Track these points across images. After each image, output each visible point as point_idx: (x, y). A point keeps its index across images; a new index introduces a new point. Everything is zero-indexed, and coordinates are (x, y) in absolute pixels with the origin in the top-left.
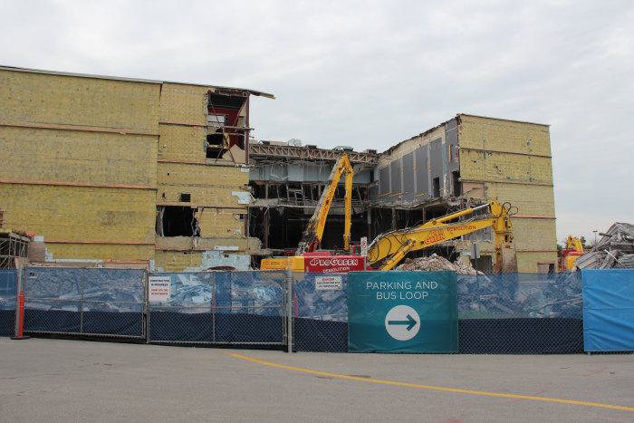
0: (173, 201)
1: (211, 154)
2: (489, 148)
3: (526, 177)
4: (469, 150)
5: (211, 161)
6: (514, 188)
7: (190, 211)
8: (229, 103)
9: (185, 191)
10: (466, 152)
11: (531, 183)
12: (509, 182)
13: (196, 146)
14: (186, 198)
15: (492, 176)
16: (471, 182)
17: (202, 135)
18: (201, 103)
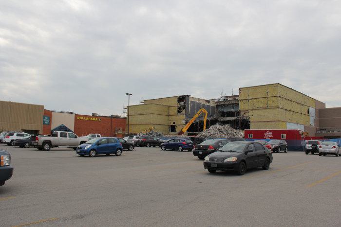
0: (172, 124)
1: (179, 112)
2: (250, 98)
3: (265, 106)
4: (243, 100)
5: (179, 114)
6: (260, 111)
7: (175, 126)
8: (181, 99)
9: (173, 121)
10: (242, 101)
11: (267, 108)
12: (258, 109)
13: (175, 111)
14: (174, 123)
15: (251, 107)
16: (243, 111)
17: (177, 108)
18: (176, 100)
